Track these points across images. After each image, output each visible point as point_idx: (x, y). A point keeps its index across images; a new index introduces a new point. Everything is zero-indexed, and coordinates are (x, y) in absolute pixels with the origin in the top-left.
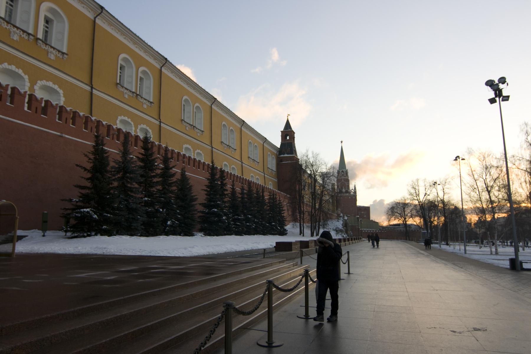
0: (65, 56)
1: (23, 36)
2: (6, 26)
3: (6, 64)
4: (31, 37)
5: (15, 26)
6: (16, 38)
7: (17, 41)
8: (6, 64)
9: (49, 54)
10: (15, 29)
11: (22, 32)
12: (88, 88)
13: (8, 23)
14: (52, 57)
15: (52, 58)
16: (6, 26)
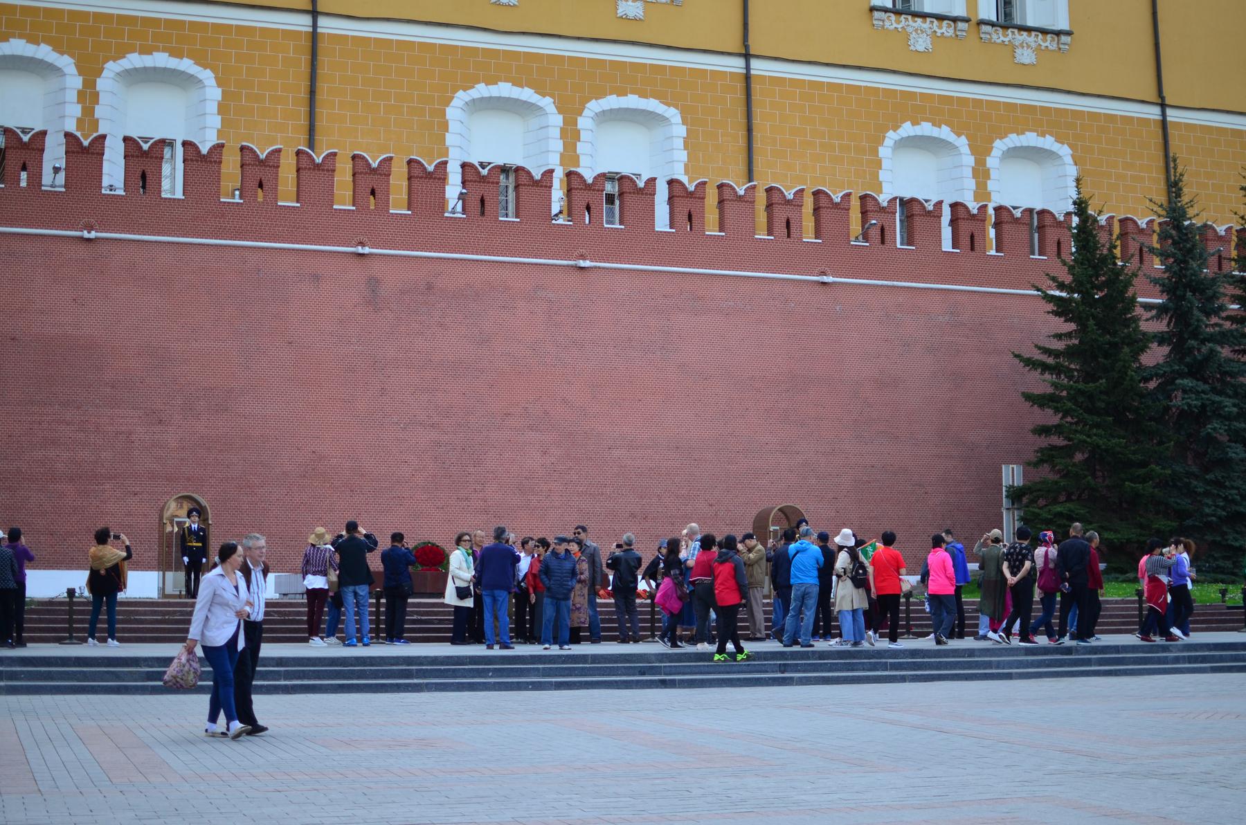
0: (1064, 38)
1: (939, 32)
2: (895, 25)
3: (907, 125)
4: (961, 25)
5: (916, 15)
6: (921, 43)
7: (926, 52)
8: (907, 125)
9: (1019, 51)
10: (919, 20)
11: (936, 22)
12: (1153, 112)
13: (898, 13)
14: (1026, 56)
15: (1027, 61)
16: (895, 25)
